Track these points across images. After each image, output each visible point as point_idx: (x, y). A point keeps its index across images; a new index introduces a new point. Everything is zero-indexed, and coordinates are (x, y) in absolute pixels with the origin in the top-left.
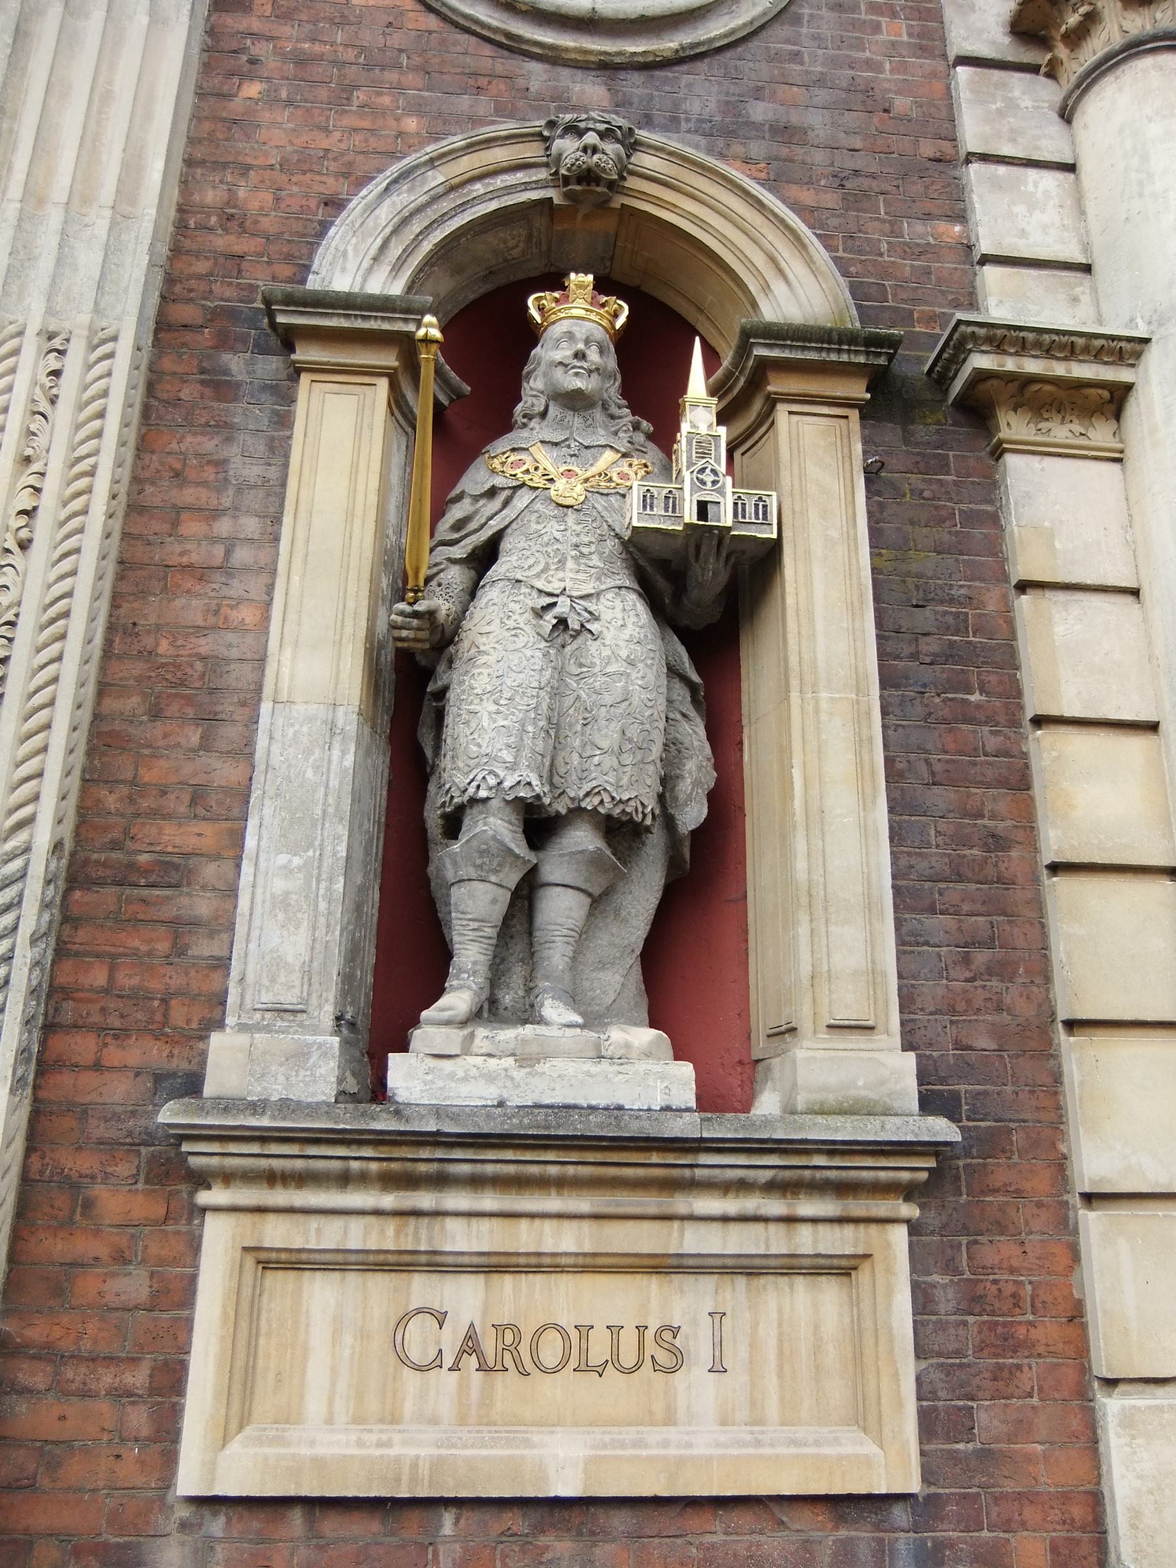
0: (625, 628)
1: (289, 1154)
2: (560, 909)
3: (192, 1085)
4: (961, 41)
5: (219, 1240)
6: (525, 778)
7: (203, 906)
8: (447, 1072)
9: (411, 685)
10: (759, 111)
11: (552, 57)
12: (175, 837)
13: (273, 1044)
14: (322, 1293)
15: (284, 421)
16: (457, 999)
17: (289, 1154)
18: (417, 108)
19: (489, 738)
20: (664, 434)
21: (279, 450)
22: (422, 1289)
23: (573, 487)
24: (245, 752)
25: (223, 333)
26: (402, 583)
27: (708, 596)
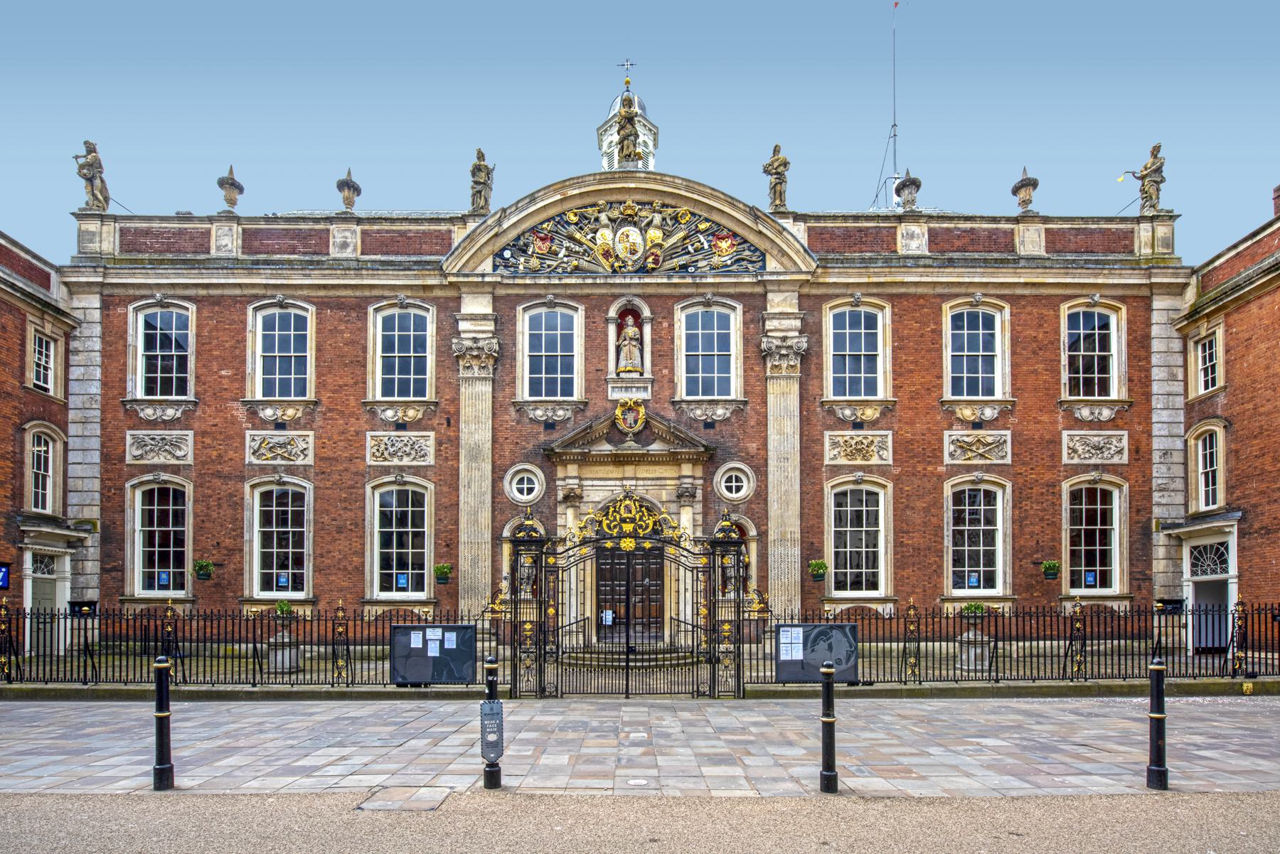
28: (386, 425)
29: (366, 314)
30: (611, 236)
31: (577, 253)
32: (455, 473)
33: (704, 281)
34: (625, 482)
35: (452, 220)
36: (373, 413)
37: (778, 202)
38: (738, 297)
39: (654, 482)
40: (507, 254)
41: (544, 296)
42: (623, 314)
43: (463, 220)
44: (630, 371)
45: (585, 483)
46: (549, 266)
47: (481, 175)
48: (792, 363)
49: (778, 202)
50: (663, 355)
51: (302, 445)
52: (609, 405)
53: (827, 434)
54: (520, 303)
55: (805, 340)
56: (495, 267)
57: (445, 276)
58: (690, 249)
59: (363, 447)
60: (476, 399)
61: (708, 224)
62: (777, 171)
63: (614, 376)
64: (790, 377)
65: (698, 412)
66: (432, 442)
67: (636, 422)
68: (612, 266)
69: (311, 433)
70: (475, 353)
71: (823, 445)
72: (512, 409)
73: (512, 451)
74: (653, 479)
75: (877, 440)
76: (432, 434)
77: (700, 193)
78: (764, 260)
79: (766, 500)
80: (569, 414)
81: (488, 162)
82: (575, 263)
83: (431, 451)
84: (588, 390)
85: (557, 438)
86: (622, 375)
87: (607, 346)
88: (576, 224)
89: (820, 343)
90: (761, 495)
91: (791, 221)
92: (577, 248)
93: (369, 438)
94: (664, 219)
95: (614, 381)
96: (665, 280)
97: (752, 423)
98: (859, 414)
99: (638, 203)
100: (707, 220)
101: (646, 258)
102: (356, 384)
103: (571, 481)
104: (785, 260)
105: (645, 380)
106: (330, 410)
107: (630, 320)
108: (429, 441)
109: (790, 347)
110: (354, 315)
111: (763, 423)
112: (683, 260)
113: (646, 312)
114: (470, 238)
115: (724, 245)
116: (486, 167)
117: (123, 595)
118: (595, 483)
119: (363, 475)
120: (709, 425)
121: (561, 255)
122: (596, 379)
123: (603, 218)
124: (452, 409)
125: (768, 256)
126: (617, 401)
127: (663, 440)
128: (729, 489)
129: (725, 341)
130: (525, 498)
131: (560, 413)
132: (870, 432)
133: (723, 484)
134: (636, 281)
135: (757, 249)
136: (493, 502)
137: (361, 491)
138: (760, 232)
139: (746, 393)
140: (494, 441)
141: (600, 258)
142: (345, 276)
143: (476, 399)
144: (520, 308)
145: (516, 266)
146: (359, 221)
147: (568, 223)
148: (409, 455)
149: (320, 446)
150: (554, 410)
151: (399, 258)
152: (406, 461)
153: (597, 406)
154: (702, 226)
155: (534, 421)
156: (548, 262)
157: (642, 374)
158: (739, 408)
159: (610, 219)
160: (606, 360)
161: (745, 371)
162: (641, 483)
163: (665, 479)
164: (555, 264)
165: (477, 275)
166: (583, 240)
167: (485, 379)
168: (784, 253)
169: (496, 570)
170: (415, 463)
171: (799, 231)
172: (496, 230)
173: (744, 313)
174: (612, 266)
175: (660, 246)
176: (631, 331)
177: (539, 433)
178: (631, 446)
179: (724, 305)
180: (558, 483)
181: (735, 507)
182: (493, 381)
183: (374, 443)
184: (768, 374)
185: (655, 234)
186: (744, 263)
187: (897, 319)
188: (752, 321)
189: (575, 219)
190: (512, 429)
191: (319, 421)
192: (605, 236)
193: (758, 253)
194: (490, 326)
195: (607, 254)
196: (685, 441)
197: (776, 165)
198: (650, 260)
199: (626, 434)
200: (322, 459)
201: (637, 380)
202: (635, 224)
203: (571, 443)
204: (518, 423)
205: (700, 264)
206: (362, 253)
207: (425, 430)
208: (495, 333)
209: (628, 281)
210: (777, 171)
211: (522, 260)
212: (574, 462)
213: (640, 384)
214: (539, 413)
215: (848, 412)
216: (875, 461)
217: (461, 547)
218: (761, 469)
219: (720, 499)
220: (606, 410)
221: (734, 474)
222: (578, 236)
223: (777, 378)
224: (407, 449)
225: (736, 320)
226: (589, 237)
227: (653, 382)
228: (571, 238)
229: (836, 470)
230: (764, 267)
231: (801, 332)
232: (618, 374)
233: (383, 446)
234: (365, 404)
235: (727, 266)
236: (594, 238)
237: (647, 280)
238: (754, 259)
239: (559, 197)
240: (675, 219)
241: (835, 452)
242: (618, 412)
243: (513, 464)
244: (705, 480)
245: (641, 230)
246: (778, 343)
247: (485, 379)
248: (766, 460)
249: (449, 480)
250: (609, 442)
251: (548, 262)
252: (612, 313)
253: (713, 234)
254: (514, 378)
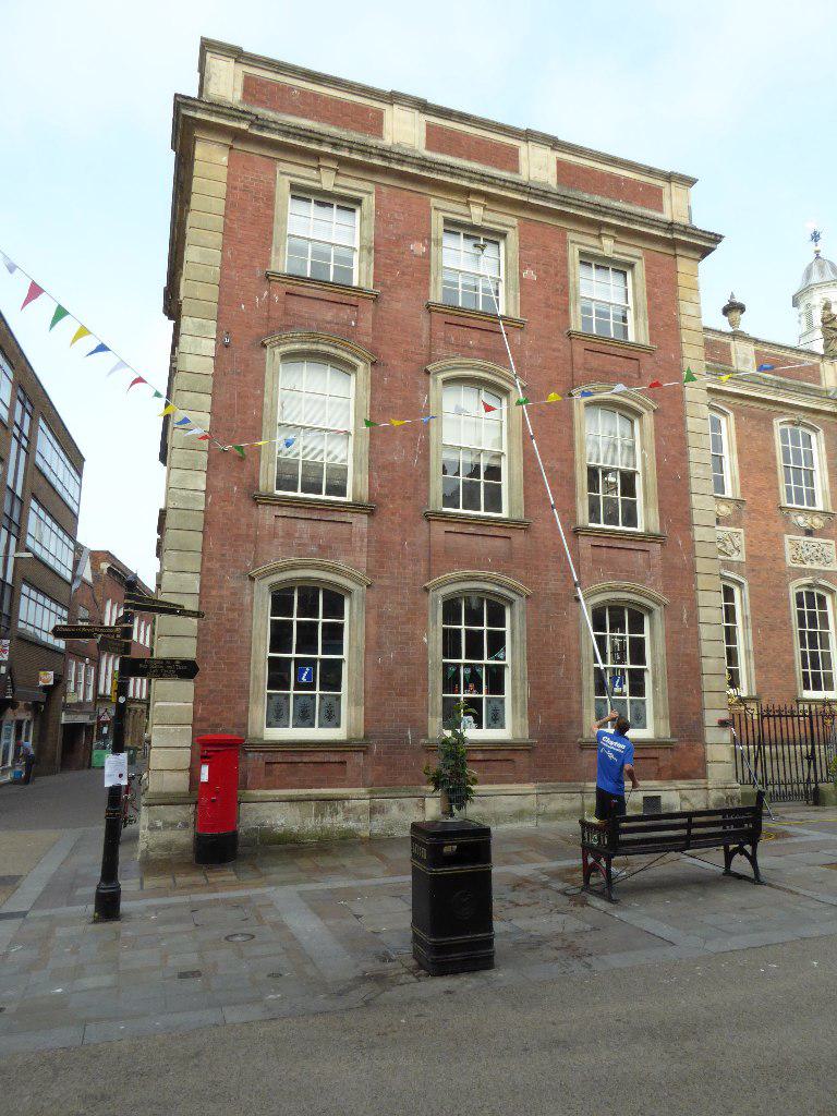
36: (787, 518)
51: (737, 543)
59: (783, 547)
69: (741, 530)
93: (786, 541)
102: (770, 489)
106: (754, 511)
110: (763, 425)
117: (426, 736)
142: (766, 391)
149: (750, 545)
152: (816, 566)
170: (823, 568)
183: (790, 545)
191: (745, 521)
200: (751, 556)
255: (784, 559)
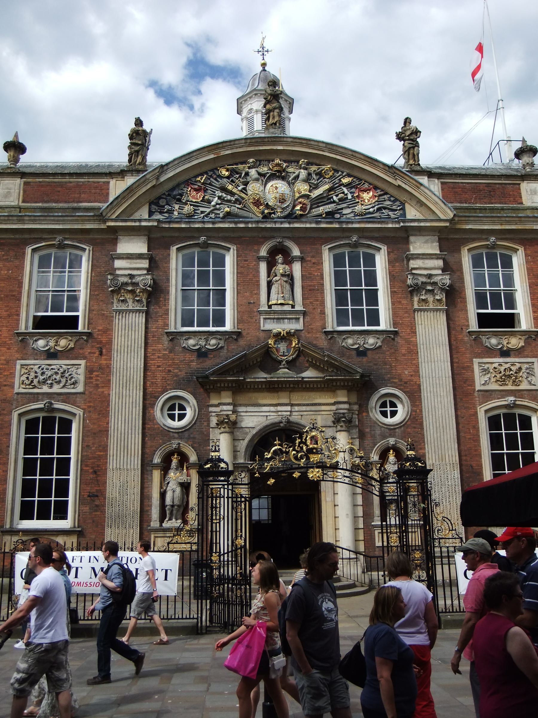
0: (178, 490)
1: (156, 530)
2: (174, 512)
3: (150, 526)
4: (212, 426)
5: (152, 536)
6: (171, 503)
7: (149, 513)
8: (166, 524)
9: (163, 495)
10: (192, 436)
11: (173, 432)
12: (147, 508)
13: (155, 523)
14: (159, 539)
15: (152, 473)
16: (167, 519)
17: (156, 530)
18: (161, 439)
19: (168, 500)
20: (183, 470)
21: (152, 476)
22: (165, 538)
23: (175, 477)
24: (151, 502)
25: (146, 466)
26: (161, 487)
27: (185, 487)
28: (37, 354)
29: (24, 253)
30: (262, 188)
31: (229, 201)
32: (105, 401)
33: (350, 226)
34: (279, 408)
35: (111, 175)
37: (411, 162)
38: (383, 240)
39: (308, 408)
40: (162, 202)
41: (198, 238)
42: (273, 252)
43: (122, 173)
44: (281, 304)
45: (240, 409)
46: (202, 212)
47: (139, 138)
48: (438, 297)
49: (411, 162)
50: (313, 290)
52: (262, 335)
53: (476, 361)
54: (173, 243)
55: (448, 277)
56: (151, 213)
57: (105, 221)
58: (335, 198)
59: (13, 375)
60: (128, 332)
61: (351, 179)
62: (409, 137)
63: (266, 308)
64: (437, 310)
65: (350, 341)
66: (82, 370)
67: (288, 351)
68: (263, 213)
70: (130, 288)
71: (473, 371)
72: (165, 338)
73: (163, 378)
74: (308, 405)
75: (525, 366)
76: (83, 362)
77: (342, 154)
78: (403, 209)
79: (421, 424)
80: (222, 343)
81: (146, 127)
82: (227, 209)
83: (81, 378)
84: (239, 321)
85: (211, 365)
86: (274, 308)
87: (258, 281)
88: (228, 177)
89: (462, 279)
90: (415, 421)
91: (426, 178)
92: (229, 197)
93: (18, 367)
94: (309, 174)
95: (266, 312)
96: (314, 225)
97: (403, 351)
98: (505, 344)
99: (285, 161)
100: (349, 175)
101: (294, 206)
102: (9, 316)
103: (225, 408)
104: (423, 209)
105: (297, 312)
107: (280, 258)
108: (79, 369)
109: (435, 283)
111: (413, 352)
112: (330, 207)
113: (296, 252)
114: (130, 190)
115: (366, 196)
116: (144, 131)
118: (250, 409)
119: (9, 403)
120: (362, 353)
121: (213, 203)
122: (248, 310)
123: (253, 172)
124: (104, 339)
125: (407, 206)
126: (270, 331)
127: (316, 367)
128: (384, 414)
129: (371, 278)
130: (176, 424)
131: (213, 342)
132: (517, 360)
133: (378, 409)
134: (287, 225)
135: (396, 200)
136: (144, 428)
137: (7, 418)
138: (399, 186)
139: (395, 324)
140: (146, 368)
141: (251, 206)
143: (128, 332)
144: (174, 249)
145: (170, 212)
146: (23, 175)
147: (221, 177)
148: (59, 382)
150: (207, 340)
151: (61, 205)
152: (56, 389)
153: (250, 337)
154: (345, 181)
155: (186, 349)
156: (202, 209)
157: (293, 307)
158: (390, 336)
159: (259, 174)
160: (258, 294)
161: (393, 304)
162: (296, 408)
163: (320, 404)
164: (208, 210)
165: (135, 221)
166: (235, 190)
167: (139, 311)
168: (421, 204)
169: (144, 498)
171: (435, 186)
172: (154, 183)
173: (389, 253)
174: (263, 213)
175: (307, 196)
176: (280, 268)
177: (192, 361)
178: (283, 373)
179: (369, 246)
180: (211, 409)
181: (392, 430)
182: (147, 313)
184: (416, 306)
185: (303, 188)
186: (384, 211)
187: (530, 260)
188: (396, 260)
189: (227, 174)
190: (165, 357)
192: (254, 188)
193: (398, 203)
194: (145, 264)
195: (257, 203)
196: (339, 368)
197: (408, 133)
198: (298, 208)
199: (280, 362)
201: (290, 312)
202: (283, 178)
203: (224, 371)
204: (170, 352)
205: (345, 211)
206: (23, 202)
207: (76, 358)
208: (149, 270)
209: (278, 225)
210: (409, 137)
211: (177, 207)
212: (227, 389)
213: (293, 315)
214: (191, 342)
215: (494, 341)
216: (524, 386)
217: (109, 474)
218: (415, 395)
219: (375, 423)
220: (258, 339)
221: (388, 400)
222: (230, 187)
223: (424, 310)
224: (58, 377)
225: (381, 262)
226: (240, 188)
227: (304, 313)
228: (224, 189)
229: (488, 395)
230: (404, 215)
231: (444, 270)
232: (270, 307)
233: (32, 375)
234: (19, 334)
235: (370, 213)
236: (244, 189)
237: (297, 225)
238: (394, 207)
239: (212, 156)
240: (320, 174)
241: (486, 378)
242: (271, 342)
243: (165, 391)
244: (360, 406)
245: (289, 183)
246: (424, 280)
247: (139, 311)
248: (419, 386)
249: (99, 407)
250: (264, 370)
251: (202, 209)
252: (263, 252)
253: (356, 187)
254: (167, 310)
255: (13, 387)
